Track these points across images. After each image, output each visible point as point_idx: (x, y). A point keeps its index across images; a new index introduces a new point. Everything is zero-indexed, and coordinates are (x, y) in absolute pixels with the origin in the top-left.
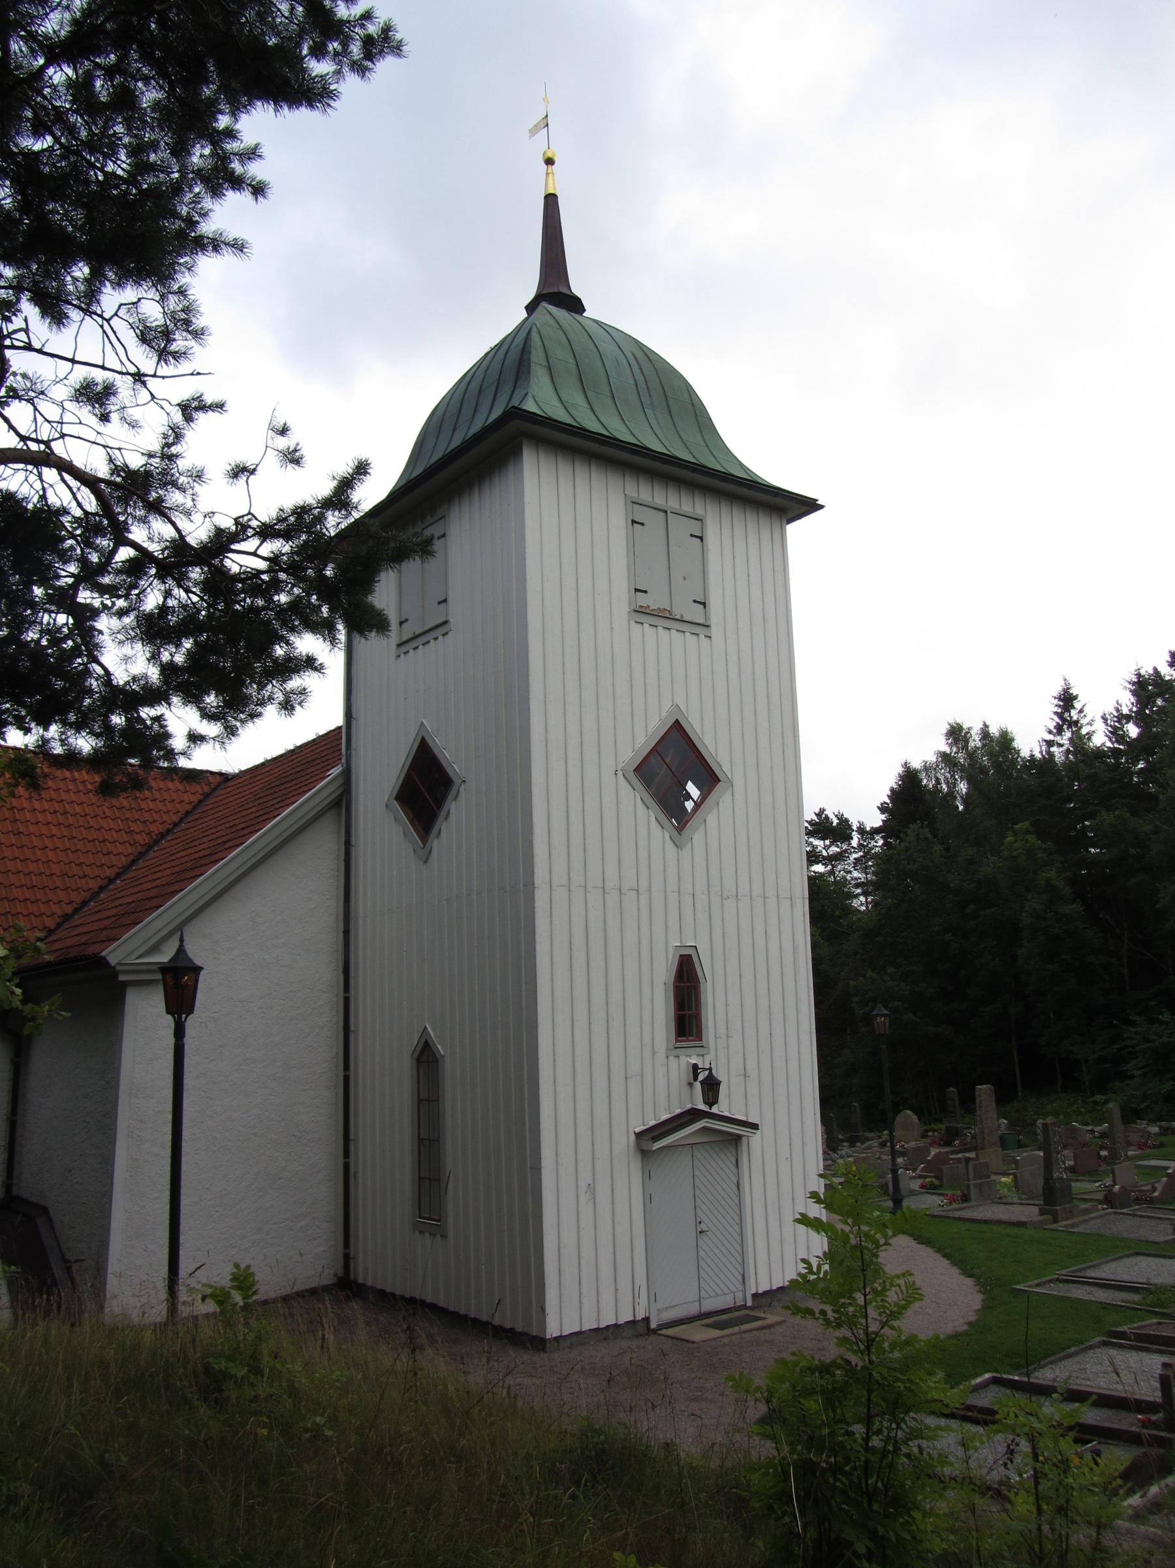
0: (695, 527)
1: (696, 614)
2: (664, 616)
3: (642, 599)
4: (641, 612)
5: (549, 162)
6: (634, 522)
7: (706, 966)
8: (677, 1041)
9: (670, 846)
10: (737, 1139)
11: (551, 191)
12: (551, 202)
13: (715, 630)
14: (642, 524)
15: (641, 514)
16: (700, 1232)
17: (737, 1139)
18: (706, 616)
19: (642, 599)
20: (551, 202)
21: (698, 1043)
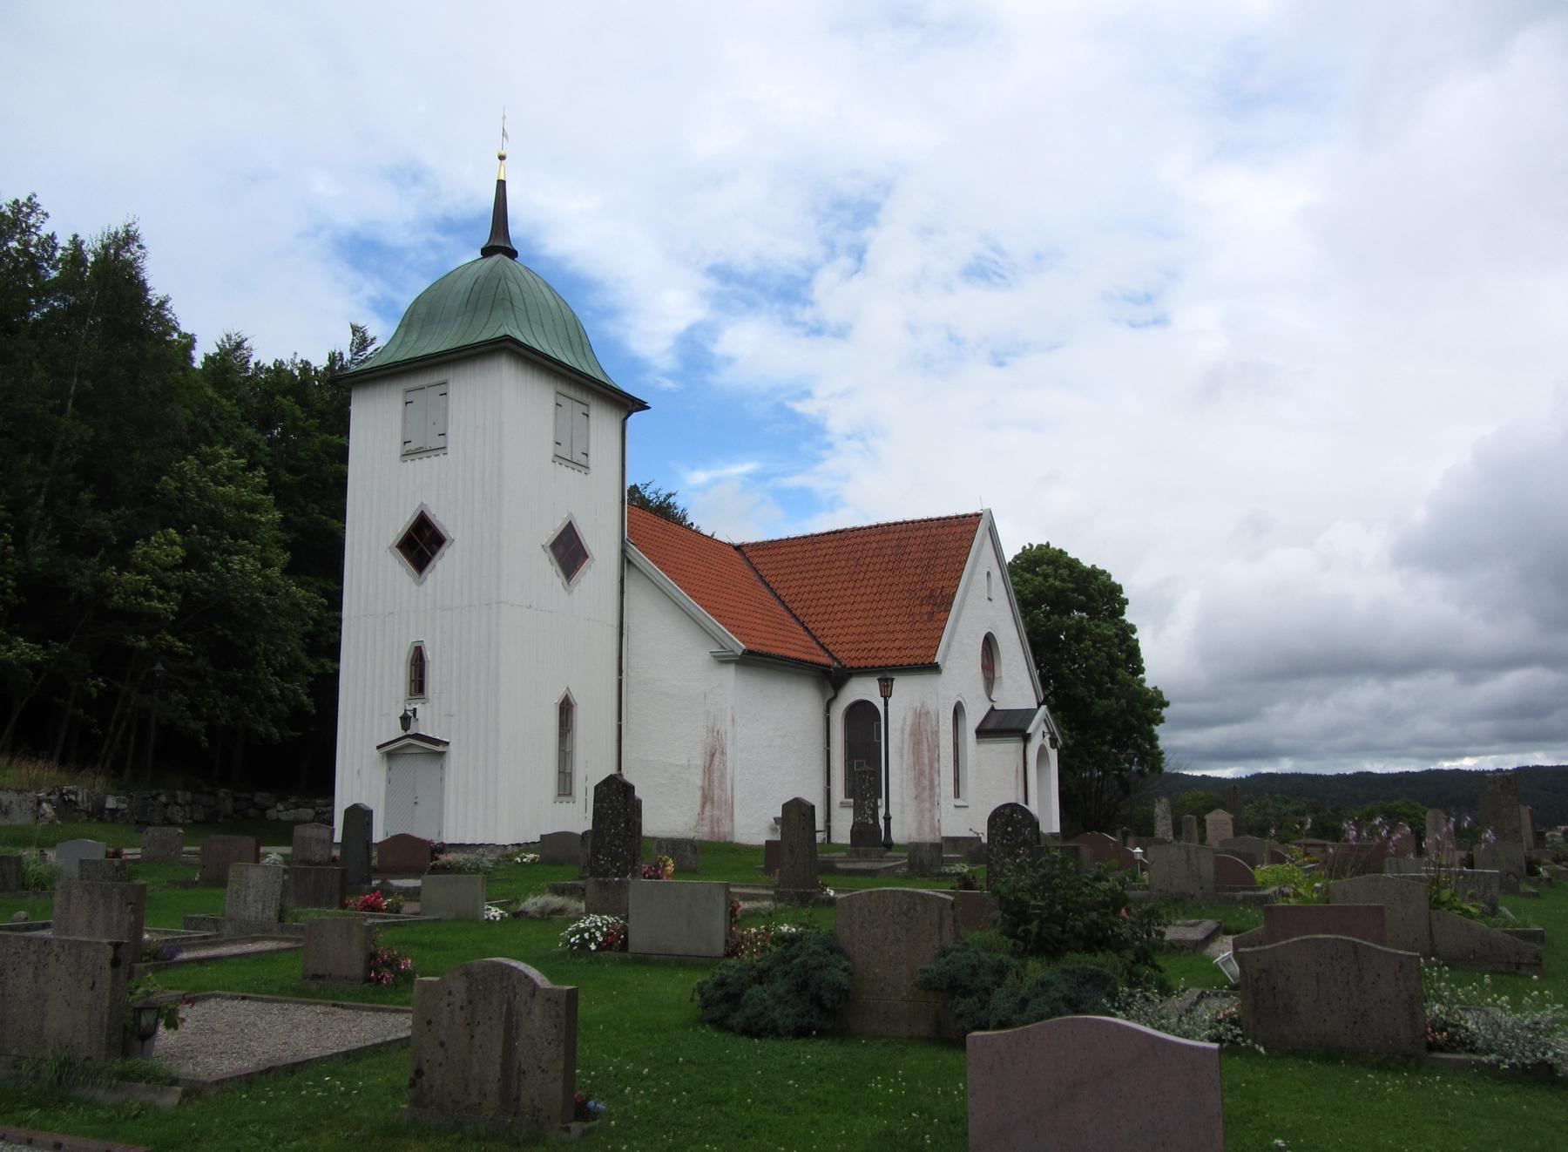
0: (442, 389)
1: (439, 442)
2: (420, 452)
3: (408, 447)
4: (407, 455)
5: (502, 158)
6: (407, 403)
7: (428, 655)
8: (411, 694)
9: (414, 587)
10: (443, 753)
11: (502, 178)
12: (501, 185)
13: (449, 449)
14: (411, 402)
15: (410, 397)
16: (416, 803)
17: (443, 753)
18: (446, 442)
19: (408, 447)
20: (501, 185)
21: (420, 697)
